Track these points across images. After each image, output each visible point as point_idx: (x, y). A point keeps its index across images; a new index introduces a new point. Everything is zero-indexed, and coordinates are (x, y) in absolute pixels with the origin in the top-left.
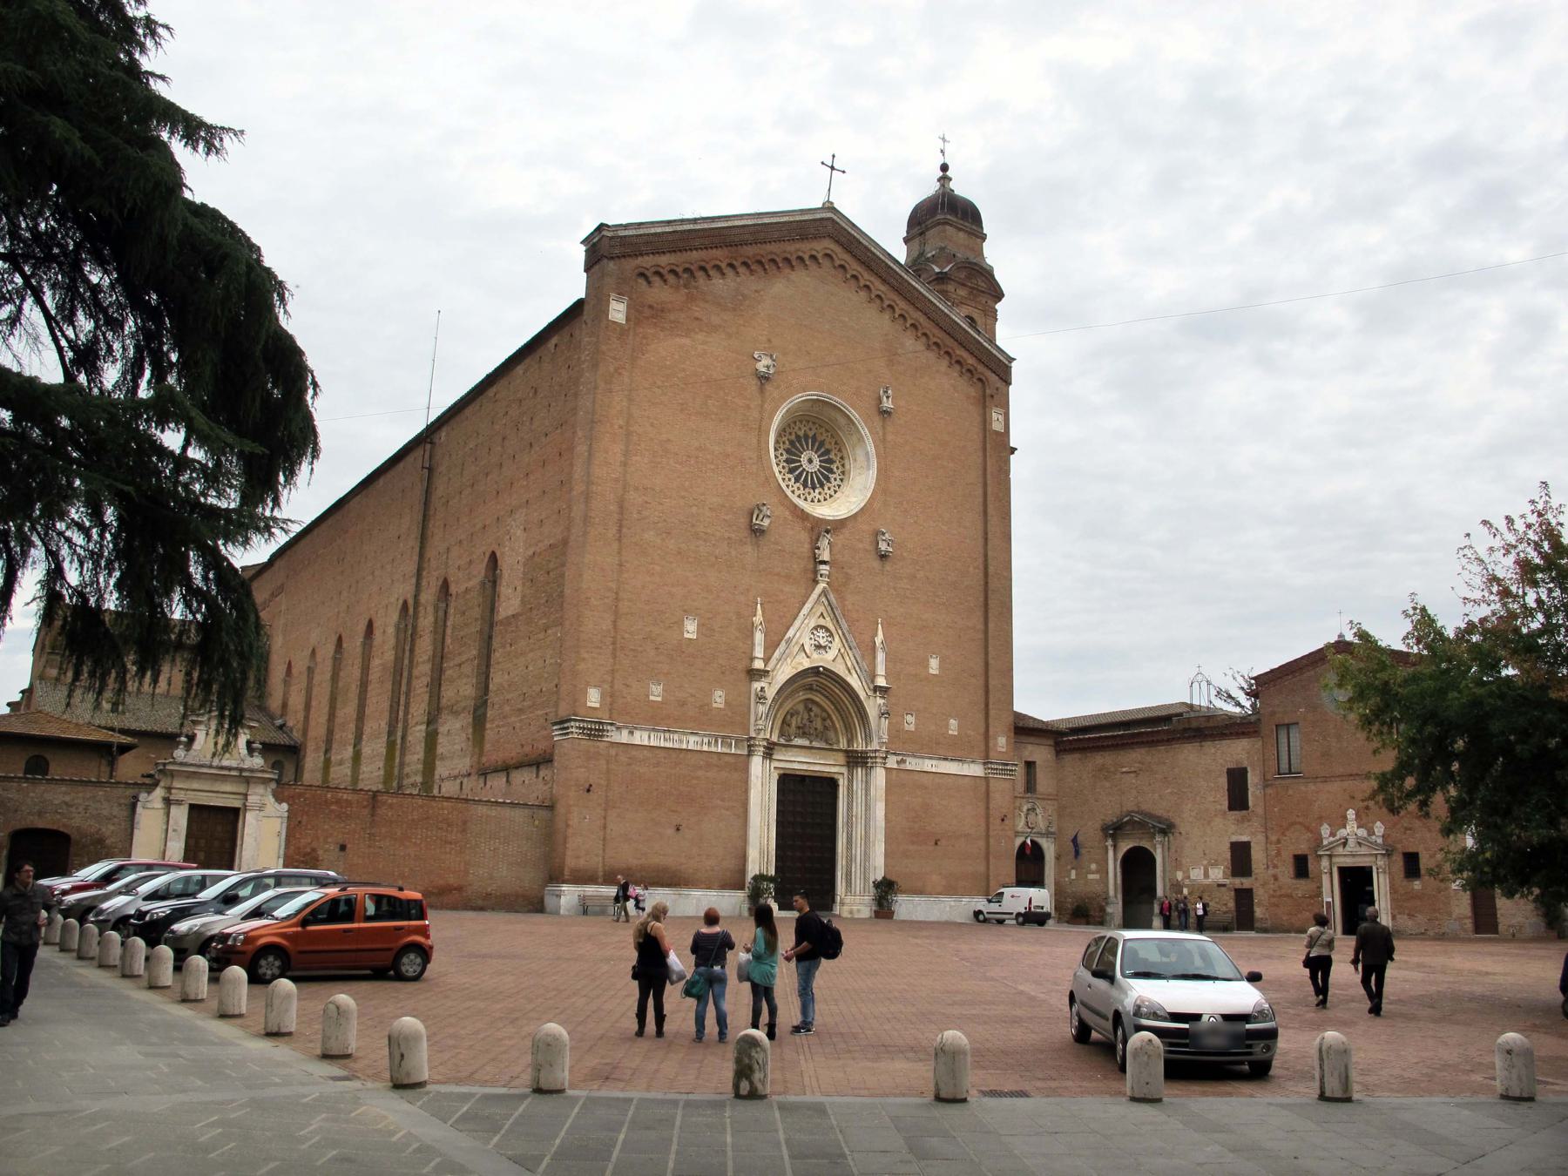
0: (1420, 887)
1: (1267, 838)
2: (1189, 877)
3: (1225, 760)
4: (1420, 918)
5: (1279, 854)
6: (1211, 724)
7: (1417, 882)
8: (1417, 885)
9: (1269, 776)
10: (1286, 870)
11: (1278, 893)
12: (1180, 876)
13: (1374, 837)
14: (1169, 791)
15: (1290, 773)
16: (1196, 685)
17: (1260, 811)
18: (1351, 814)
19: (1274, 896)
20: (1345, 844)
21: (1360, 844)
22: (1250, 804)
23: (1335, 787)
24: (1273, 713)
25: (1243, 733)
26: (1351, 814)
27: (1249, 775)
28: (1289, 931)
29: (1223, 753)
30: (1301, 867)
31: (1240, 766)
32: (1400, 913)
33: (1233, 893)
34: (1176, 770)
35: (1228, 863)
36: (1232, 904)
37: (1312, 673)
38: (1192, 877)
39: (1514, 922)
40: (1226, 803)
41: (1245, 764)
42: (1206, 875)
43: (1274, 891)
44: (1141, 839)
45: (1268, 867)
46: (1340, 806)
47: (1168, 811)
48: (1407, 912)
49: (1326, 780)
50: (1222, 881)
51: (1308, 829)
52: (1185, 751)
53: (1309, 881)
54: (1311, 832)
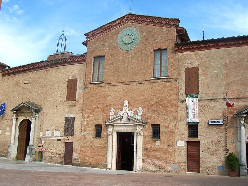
4: (157, 162)
5: (87, 124)
8: (158, 143)
10: (91, 132)
11: (85, 145)
12: (41, 134)
13: (137, 116)
16: (61, 40)
17: (81, 101)
18: (126, 103)
19: (83, 147)
20: (121, 119)
21: (129, 119)
22: (77, 98)
23: (119, 88)
24: (93, 51)
25: (78, 61)
26: (126, 103)
27: (78, 83)
30: (99, 131)
33: (64, 144)
35: (63, 129)
36: (63, 150)
37: (114, 30)
38: (46, 135)
39: (209, 165)
42: (53, 134)
46: (121, 99)
49: (116, 84)
50: (59, 138)
51: (103, 111)
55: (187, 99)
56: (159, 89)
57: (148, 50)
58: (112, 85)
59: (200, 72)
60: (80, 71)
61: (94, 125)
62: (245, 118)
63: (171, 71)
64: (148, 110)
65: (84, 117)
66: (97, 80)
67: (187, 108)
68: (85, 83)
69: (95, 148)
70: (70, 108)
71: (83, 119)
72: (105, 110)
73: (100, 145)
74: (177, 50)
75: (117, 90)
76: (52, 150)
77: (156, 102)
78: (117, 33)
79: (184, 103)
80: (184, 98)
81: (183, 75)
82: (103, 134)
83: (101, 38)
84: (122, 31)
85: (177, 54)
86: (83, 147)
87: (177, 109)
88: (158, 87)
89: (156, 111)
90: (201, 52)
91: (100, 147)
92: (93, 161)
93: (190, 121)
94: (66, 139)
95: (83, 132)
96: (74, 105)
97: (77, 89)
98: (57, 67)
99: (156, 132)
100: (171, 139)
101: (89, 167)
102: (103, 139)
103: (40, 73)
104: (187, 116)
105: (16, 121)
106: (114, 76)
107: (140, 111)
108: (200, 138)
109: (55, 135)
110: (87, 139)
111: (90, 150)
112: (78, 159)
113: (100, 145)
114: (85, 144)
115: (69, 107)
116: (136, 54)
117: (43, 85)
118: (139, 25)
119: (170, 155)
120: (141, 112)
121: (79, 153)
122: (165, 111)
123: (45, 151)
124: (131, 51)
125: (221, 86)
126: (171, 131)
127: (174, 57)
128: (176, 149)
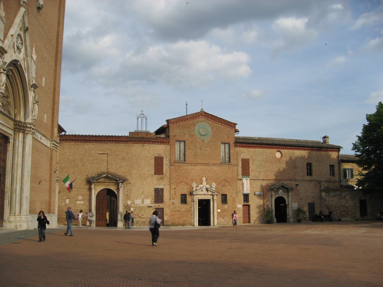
2: (134, 203)
3: (154, 153)
5: (175, 194)
6: (148, 137)
7: (226, 205)
8: (226, 206)
9: (172, 162)
10: (178, 200)
11: (174, 210)
12: (129, 202)
14: (125, 164)
16: (140, 119)
17: (168, 175)
18: (204, 179)
19: (172, 211)
22: (164, 172)
23: (198, 168)
25: (163, 142)
26: (204, 179)
27: (164, 160)
28: (178, 226)
29: (153, 149)
31: (160, 156)
32: (219, 217)
34: (130, 155)
35: (153, 197)
37: (191, 122)
38: (136, 203)
40: (153, 171)
41: (163, 155)
42: (143, 202)
43: (173, 209)
44: (109, 185)
46: (200, 176)
47: (124, 173)
48: (222, 216)
49: (195, 164)
51: (187, 184)
52: (135, 147)
53: (187, 205)
55: (243, 179)
59: (250, 162)
61: (180, 194)
62: (275, 191)
64: (219, 184)
67: (243, 184)
68: (170, 161)
69: (183, 211)
70: (158, 181)
72: (188, 183)
74: (237, 145)
76: (143, 215)
77: (224, 179)
78: (194, 126)
79: (241, 181)
80: (241, 178)
81: (240, 163)
84: (198, 124)
87: (237, 185)
89: (224, 186)
90: (250, 149)
91: (186, 211)
92: (181, 221)
93: (245, 192)
94: (157, 205)
95: (171, 200)
96: (162, 179)
97: (164, 165)
98: (142, 144)
99: (224, 199)
101: (178, 225)
103: (121, 146)
104: (243, 189)
105: (95, 190)
106: (194, 158)
107: (214, 185)
108: (250, 203)
109: (145, 203)
112: (169, 221)
113: (187, 209)
114: (174, 209)
115: (157, 180)
117: (126, 159)
118: (211, 122)
120: (215, 185)
123: (136, 217)
124: (206, 141)
125: (261, 172)
126: (234, 198)
127: (234, 150)
128: (237, 210)
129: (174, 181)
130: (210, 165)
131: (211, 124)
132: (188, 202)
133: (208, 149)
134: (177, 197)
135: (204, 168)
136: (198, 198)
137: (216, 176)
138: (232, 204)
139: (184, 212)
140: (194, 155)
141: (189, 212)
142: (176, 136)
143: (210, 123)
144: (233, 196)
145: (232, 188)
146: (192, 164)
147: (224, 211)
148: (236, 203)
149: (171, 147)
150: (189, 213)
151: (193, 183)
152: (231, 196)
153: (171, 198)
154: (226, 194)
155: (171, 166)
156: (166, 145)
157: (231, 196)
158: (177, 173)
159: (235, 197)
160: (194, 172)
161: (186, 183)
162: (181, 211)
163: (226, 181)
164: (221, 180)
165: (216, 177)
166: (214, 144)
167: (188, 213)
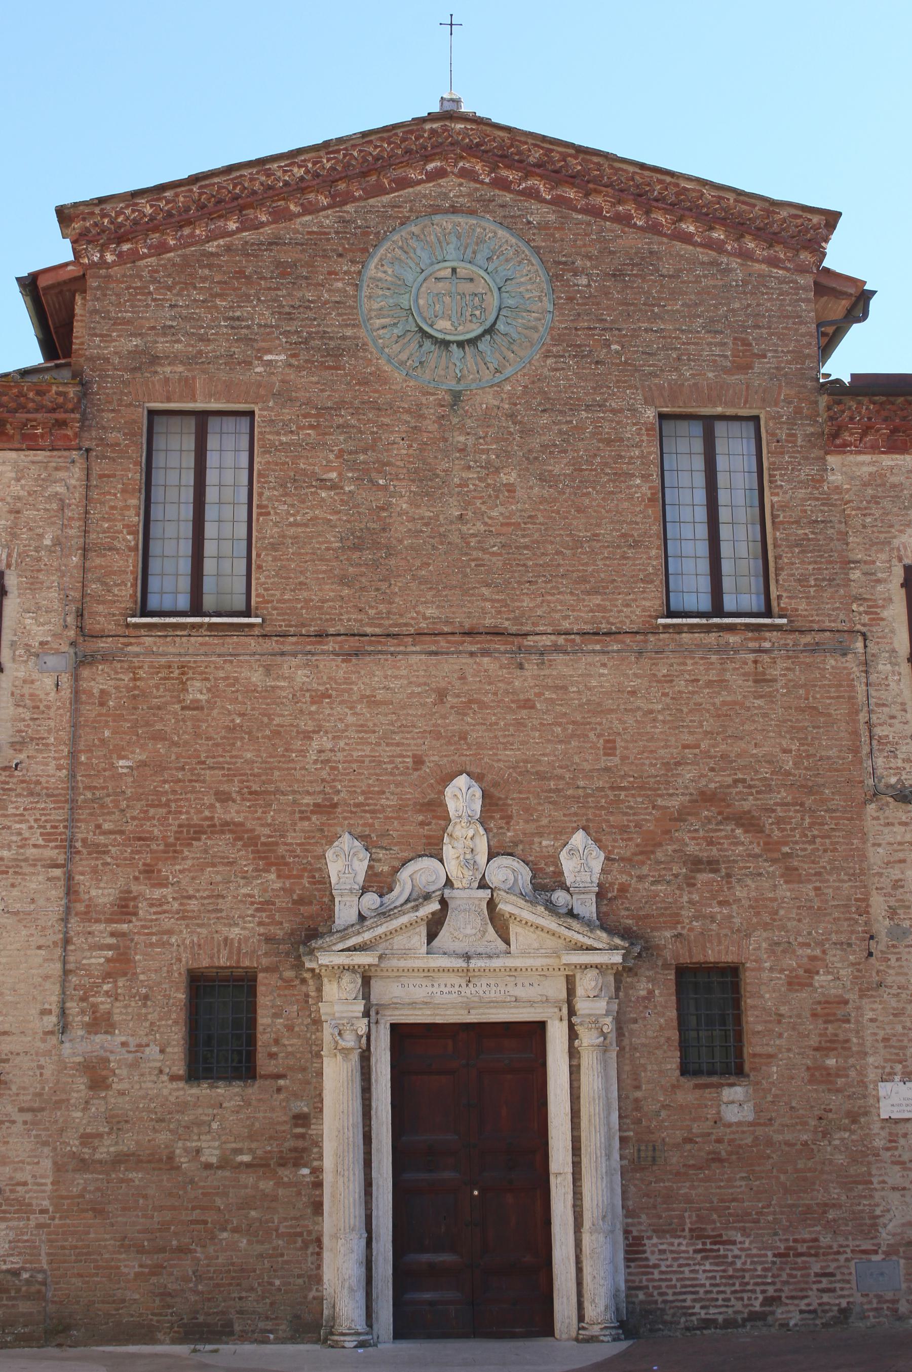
0: (747, 1114)
1: (71, 891)
7: (737, 1092)
11: (105, 1150)
13: (560, 897)
15: (196, 608)
19: (84, 1165)
28: (146, 1334)
32: (660, 1232)
37: (328, 219)
45: (64, 1027)
46: (419, 762)
53: (253, 1090)
54: (280, 864)
56: (717, 701)
57: (621, 411)
58: (331, 645)
60: (29, 513)
63: (802, 581)
64: (646, 851)
65: (81, 907)
66: (183, 602)
68: (80, 615)
69: (208, 1166)
71: (73, 920)
72: (281, 850)
73: (251, 1137)
75: (380, 695)
77: (707, 798)
82: (277, 1042)
83: (210, 266)
84: (396, 237)
85: (833, 460)
86: (84, 1165)
87: (863, 857)
88: (709, 684)
89: (712, 865)
91: (246, 1158)
100: (840, 1072)
102: (279, 1090)
106: (344, 580)
110: (122, 1093)
111: (150, 1192)
114: (100, 1136)
116: (526, 432)
118: (539, 213)
119: (835, 1192)
121: (42, 1219)
122: (774, 861)
129: (106, 826)
130: (530, 641)
131: (543, 227)
132: (272, 1056)
133: (509, 477)
134: (146, 997)
135: (462, 678)
136: (394, 1006)
137: (617, 760)
138: (811, 1081)
139: (218, 1168)
140: (356, 548)
141: (286, 1174)
142: (155, 360)
143: (534, 219)
144: (821, 979)
145: (808, 889)
146: (321, 635)
147: (716, 1159)
148: (861, 1073)
149: (96, 470)
150: (279, 1183)
151: (330, 843)
152: (794, 983)
153: (73, 1007)
154: (730, 958)
155: (85, 673)
156: (41, 455)
157: (794, 983)
158: (159, 737)
159: (852, 996)
160: (351, 719)
161: (252, 841)
162: (184, 1161)
163: (727, 819)
164: (674, 803)
165: (607, 769)
166: (579, 428)
167: (267, 1185)
